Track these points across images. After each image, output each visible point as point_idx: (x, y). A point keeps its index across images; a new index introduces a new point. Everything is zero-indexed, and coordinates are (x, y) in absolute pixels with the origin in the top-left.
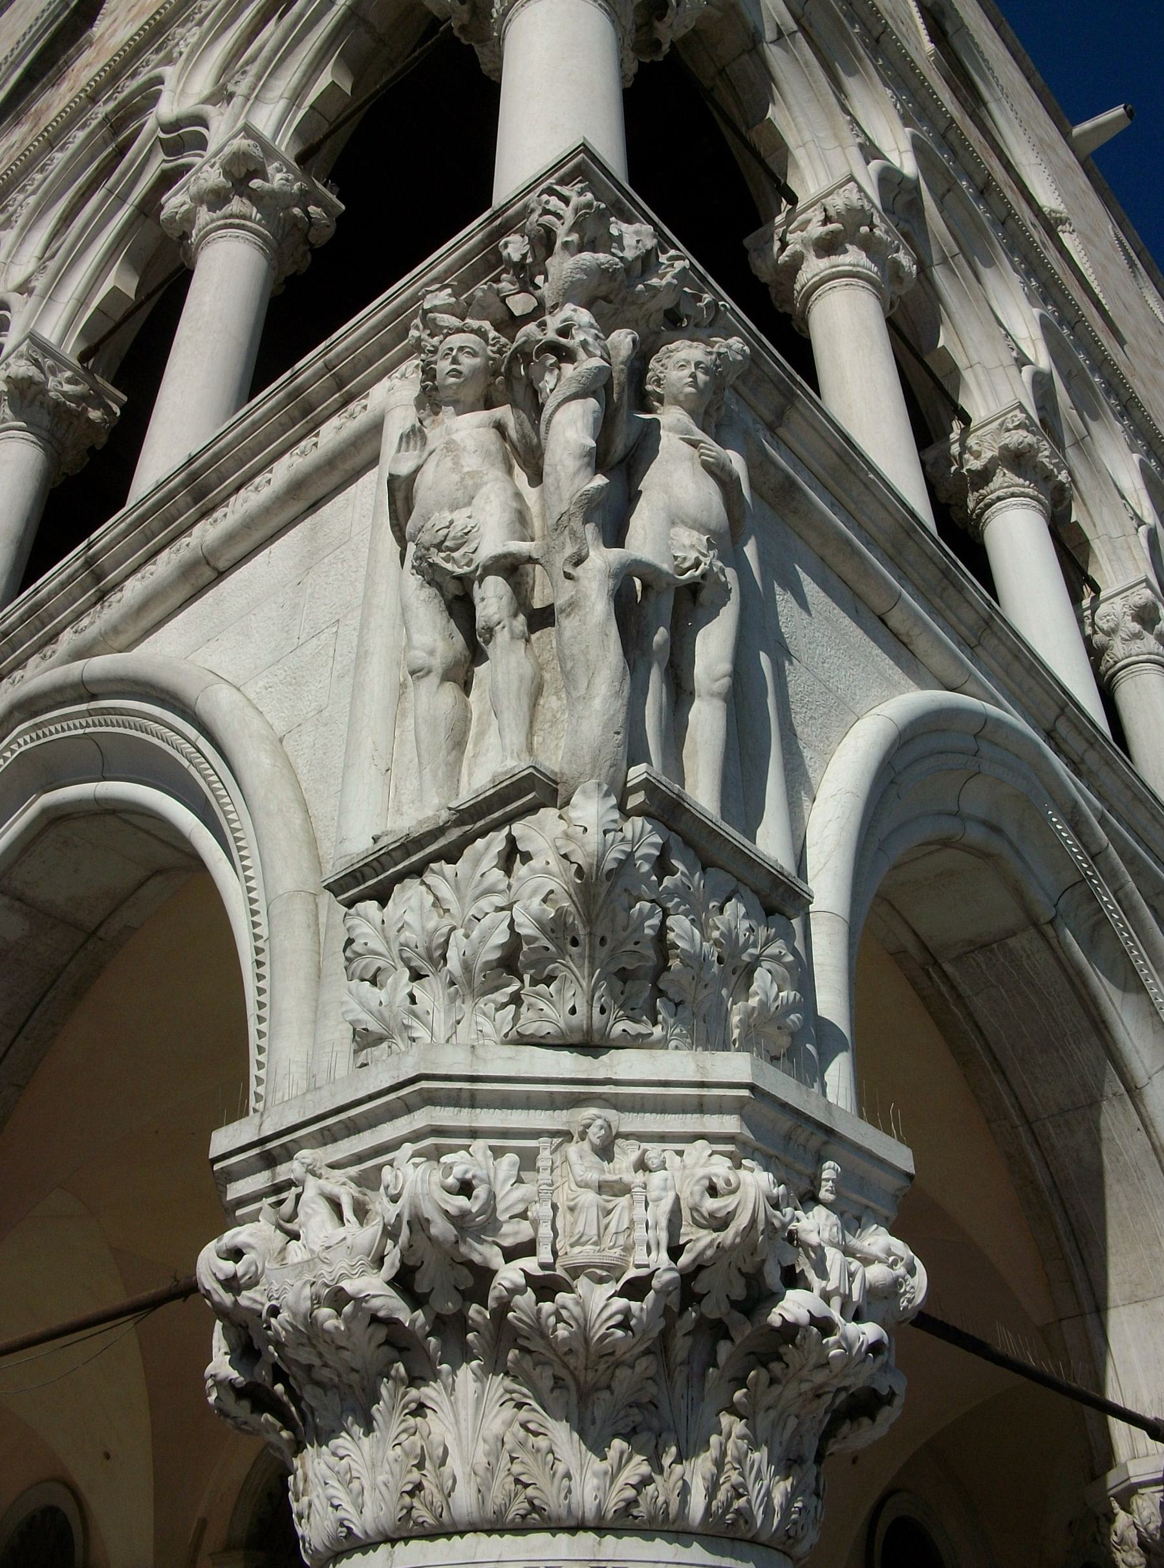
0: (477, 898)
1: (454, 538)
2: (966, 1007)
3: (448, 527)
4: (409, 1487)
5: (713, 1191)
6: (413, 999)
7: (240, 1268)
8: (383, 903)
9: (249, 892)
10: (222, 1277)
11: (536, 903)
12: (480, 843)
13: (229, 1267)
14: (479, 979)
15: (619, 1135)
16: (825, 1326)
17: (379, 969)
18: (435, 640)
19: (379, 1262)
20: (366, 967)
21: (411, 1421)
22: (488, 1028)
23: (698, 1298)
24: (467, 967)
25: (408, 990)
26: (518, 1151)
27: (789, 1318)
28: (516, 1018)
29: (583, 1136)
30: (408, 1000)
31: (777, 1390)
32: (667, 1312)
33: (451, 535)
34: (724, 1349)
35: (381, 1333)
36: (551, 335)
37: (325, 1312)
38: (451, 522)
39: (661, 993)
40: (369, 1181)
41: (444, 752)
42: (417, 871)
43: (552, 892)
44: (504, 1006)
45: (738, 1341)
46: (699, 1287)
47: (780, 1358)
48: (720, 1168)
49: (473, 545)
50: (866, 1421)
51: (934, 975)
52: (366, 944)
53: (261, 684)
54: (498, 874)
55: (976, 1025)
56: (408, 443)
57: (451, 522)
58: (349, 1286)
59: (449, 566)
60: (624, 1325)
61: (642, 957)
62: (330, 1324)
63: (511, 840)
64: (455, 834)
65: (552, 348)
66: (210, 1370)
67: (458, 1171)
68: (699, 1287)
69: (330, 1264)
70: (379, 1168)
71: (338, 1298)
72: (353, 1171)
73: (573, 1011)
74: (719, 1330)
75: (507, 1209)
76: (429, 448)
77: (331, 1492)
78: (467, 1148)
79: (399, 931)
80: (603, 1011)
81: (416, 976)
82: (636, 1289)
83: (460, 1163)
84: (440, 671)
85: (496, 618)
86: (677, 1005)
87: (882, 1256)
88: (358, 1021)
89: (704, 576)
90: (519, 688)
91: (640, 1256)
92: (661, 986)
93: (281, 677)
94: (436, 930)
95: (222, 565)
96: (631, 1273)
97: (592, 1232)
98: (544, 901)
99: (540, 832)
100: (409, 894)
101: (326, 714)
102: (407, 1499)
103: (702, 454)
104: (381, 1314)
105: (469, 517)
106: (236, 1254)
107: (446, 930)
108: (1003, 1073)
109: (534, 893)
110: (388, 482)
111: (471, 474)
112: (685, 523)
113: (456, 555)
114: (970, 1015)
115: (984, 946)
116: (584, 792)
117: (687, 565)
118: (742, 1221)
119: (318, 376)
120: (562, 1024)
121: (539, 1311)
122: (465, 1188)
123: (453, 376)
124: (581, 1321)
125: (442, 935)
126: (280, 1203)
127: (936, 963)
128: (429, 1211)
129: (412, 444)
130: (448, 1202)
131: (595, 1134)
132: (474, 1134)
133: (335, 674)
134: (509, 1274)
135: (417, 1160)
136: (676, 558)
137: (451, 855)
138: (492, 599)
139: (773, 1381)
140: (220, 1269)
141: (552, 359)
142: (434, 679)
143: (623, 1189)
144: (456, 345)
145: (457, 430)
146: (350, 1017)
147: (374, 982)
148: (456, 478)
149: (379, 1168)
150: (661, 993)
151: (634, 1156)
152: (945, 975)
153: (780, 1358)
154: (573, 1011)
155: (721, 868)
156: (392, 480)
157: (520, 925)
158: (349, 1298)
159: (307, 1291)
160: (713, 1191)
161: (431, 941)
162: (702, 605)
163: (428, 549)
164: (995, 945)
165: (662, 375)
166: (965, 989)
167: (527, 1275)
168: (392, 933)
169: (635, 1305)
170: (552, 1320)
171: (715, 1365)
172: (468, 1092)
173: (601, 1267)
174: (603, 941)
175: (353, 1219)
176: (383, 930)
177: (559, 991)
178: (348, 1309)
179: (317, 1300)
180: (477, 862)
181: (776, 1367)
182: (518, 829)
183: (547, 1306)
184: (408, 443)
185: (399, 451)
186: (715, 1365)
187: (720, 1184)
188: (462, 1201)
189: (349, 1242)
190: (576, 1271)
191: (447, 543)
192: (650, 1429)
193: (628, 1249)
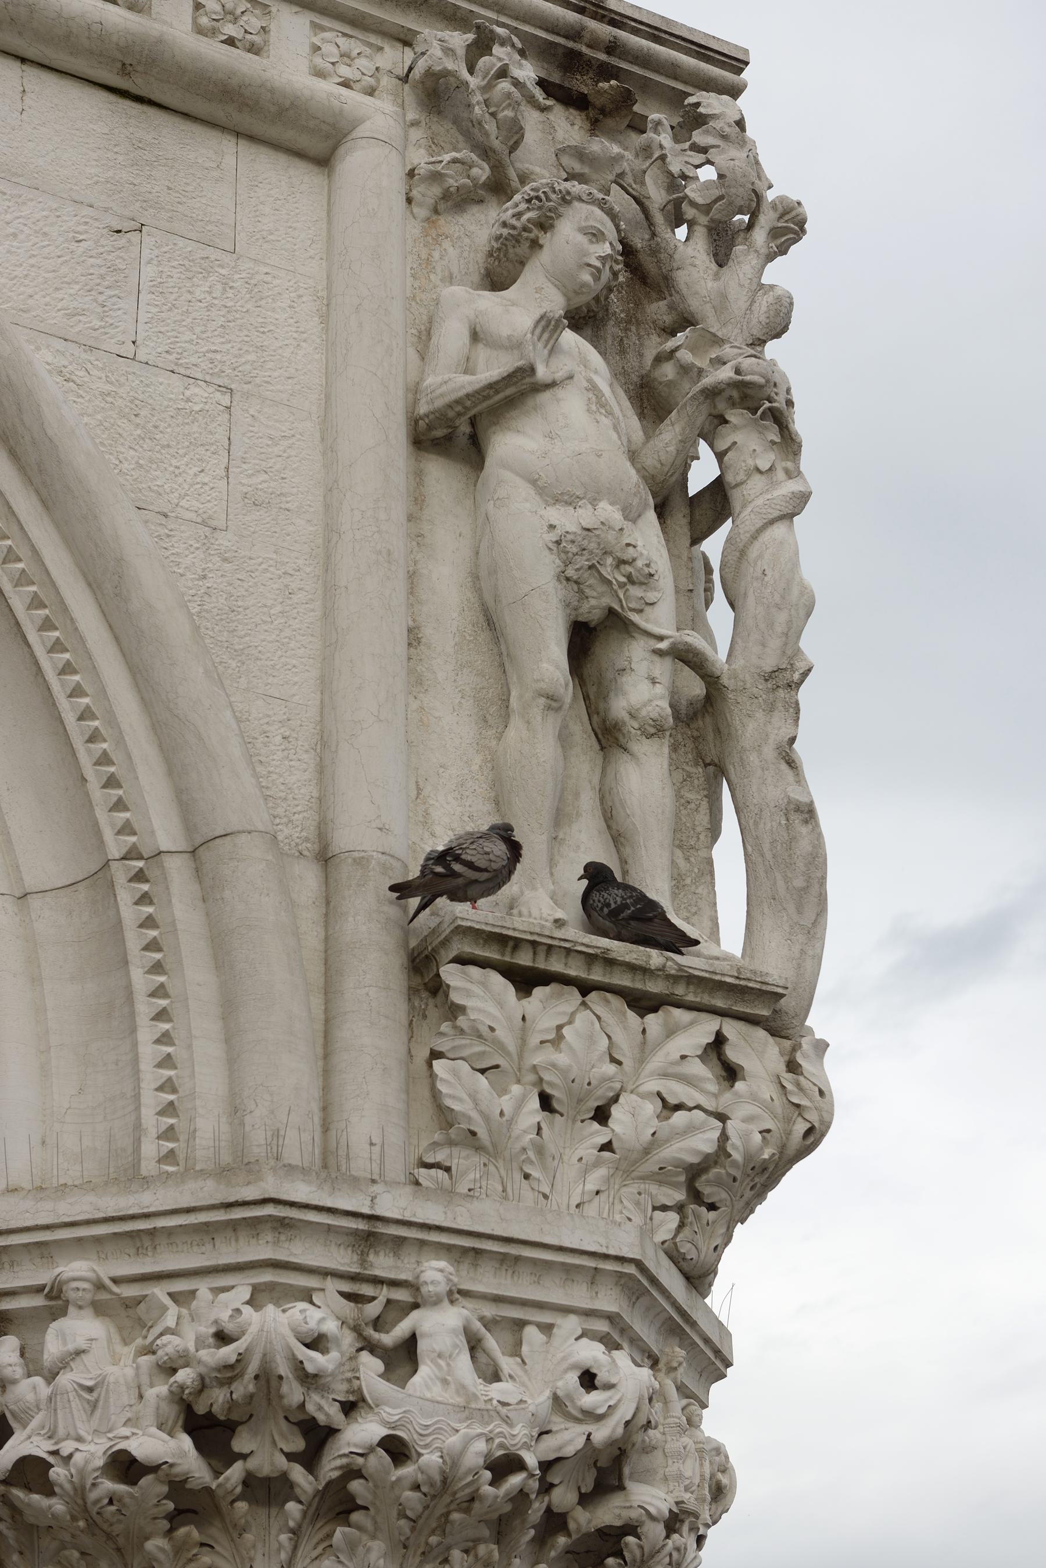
1: (639, 571)
12: (679, 1015)
42: (585, 989)
52: (492, 1029)
63: (719, 1041)
64: (655, 987)
88: (469, 1119)
94: (610, 1079)
123: (592, 274)
125: (611, 1089)
129: (546, 336)
176: (524, 1030)
191: (629, 569)
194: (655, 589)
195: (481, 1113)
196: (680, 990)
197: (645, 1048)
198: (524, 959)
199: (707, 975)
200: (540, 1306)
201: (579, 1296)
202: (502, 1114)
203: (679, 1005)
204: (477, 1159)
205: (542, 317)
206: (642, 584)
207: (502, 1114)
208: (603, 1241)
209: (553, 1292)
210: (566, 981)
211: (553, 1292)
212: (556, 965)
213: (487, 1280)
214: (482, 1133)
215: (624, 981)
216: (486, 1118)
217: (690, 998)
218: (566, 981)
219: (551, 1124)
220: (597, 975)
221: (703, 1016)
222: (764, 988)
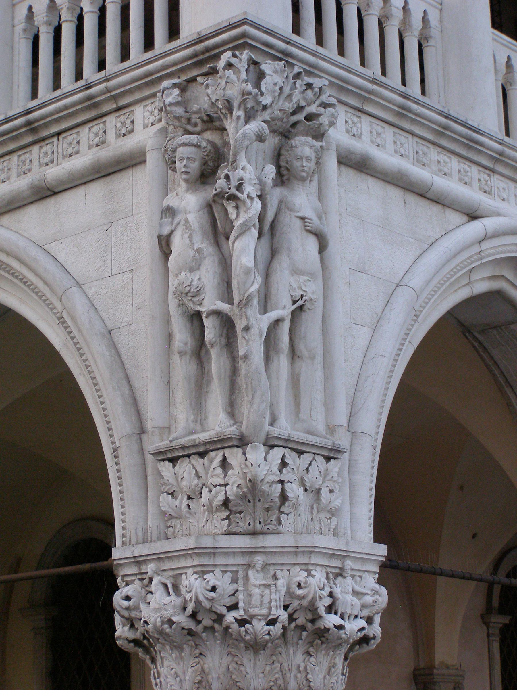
0: (212, 476)
1: (193, 292)
2: (489, 354)
3: (190, 286)
4: (197, 681)
5: (299, 586)
6: (188, 506)
7: (131, 603)
8: (174, 466)
9: (106, 417)
10: (124, 607)
11: (235, 488)
12: (212, 454)
13: (125, 603)
14: (214, 509)
15: (267, 564)
16: (340, 627)
17: (174, 491)
18: (187, 337)
19: (184, 608)
20: (169, 489)
21: (197, 660)
22: (218, 526)
23: (295, 620)
24: (211, 504)
25: (187, 503)
26: (230, 571)
27: (327, 627)
28: (229, 526)
29: (254, 567)
30: (187, 507)
31: (324, 646)
32: (284, 628)
33: (192, 290)
34: (305, 633)
35: (186, 632)
36: (233, 191)
37: (166, 626)
38: (192, 281)
39: (283, 513)
40: (177, 578)
41: (194, 393)
42: (189, 456)
43: (240, 484)
44: (224, 519)
45: (309, 632)
46: (295, 616)
47: (324, 637)
48: (302, 576)
49: (202, 297)
50: (365, 645)
51: (469, 337)
52: (168, 480)
53: (93, 289)
54: (219, 471)
55: (495, 362)
56: (166, 214)
57: (192, 281)
58: (174, 619)
59: (191, 305)
60: (269, 634)
61: (274, 503)
62: (168, 630)
65: (232, 198)
66: (117, 634)
67: (211, 583)
68: (295, 616)
69: (167, 611)
70: (182, 574)
71: (171, 622)
72: (171, 573)
73: (249, 524)
74: (303, 628)
75: (228, 593)
76: (176, 221)
77: (168, 680)
78: (213, 571)
79: (182, 479)
80: (260, 523)
81: (189, 498)
82: (272, 622)
83: (211, 579)
84: (190, 352)
85: (214, 339)
86: (288, 515)
87: (369, 592)
88: (168, 512)
89: (304, 302)
90: (225, 376)
91: (273, 612)
92: (282, 510)
93: (105, 291)
94: (197, 485)
95: (56, 191)
96: (271, 617)
97: (258, 603)
98: (238, 486)
99: (234, 457)
100: (185, 465)
101: (132, 328)
102: (197, 685)
103: (306, 226)
104: (186, 628)
105: (199, 279)
106: (128, 598)
107: (201, 486)
108: (511, 387)
109: (234, 483)
110: (158, 237)
111: (199, 251)
112: (297, 274)
113: (195, 299)
114: (492, 357)
115: (496, 327)
116: (251, 447)
117: (298, 299)
118: (310, 597)
119: (102, 93)
120: (245, 529)
121: (240, 630)
122: (214, 589)
123: (185, 174)
124: (254, 634)
125: (199, 487)
126: (144, 579)
127: (469, 332)
128: (201, 598)
130: (207, 595)
131: (259, 566)
132: (215, 565)
133: (135, 305)
134: (230, 617)
135: (196, 576)
136: (292, 296)
137: (202, 455)
138: (211, 329)
139: (322, 643)
140: (123, 604)
141: (233, 204)
142: (188, 357)
143: (268, 586)
144: (185, 156)
145: (189, 212)
146: (164, 509)
147: (172, 494)
148: (192, 253)
149: (182, 574)
150: (283, 513)
151: (272, 573)
152: (475, 337)
153: (324, 637)
154: (249, 524)
155: (307, 452)
156: (159, 237)
157: (229, 495)
158: (174, 623)
159: (159, 619)
160: (299, 586)
161: (195, 488)
162: (305, 311)
163: (182, 293)
164: (503, 327)
165: (289, 159)
166: (486, 344)
167: (236, 620)
168: (180, 479)
169: (272, 627)
170: (244, 633)
171: (301, 639)
172: (213, 552)
173: (260, 616)
174: (260, 500)
175: (173, 594)
177: (244, 517)
178: (174, 626)
179: (163, 623)
180: (211, 461)
181: (323, 639)
182: (227, 452)
183: (242, 629)
184: (166, 214)
185: (162, 218)
186: (301, 639)
187: (302, 584)
188: (212, 594)
189: (172, 604)
190: (252, 617)
191: (189, 294)
192: (279, 662)
193: (270, 609)
194: (203, 293)
195: (171, 508)
196: (208, 447)
197: (206, 469)
198: (169, 456)
199: (209, 440)
200: (183, 568)
201: (189, 562)
202: (176, 506)
203: (212, 451)
204: (178, 521)
205: (162, 212)
206: (197, 295)
207: (176, 506)
208: (186, 545)
209: (183, 563)
210: (184, 456)
211: (183, 563)
212: (177, 454)
213: (168, 565)
214: (173, 514)
215: (194, 451)
216: (173, 509)
217: (211, 448)
218: (184, 456)
219: (193, 502)
220: (187, 453)
221: (219, 451)
222: (225, 437)
